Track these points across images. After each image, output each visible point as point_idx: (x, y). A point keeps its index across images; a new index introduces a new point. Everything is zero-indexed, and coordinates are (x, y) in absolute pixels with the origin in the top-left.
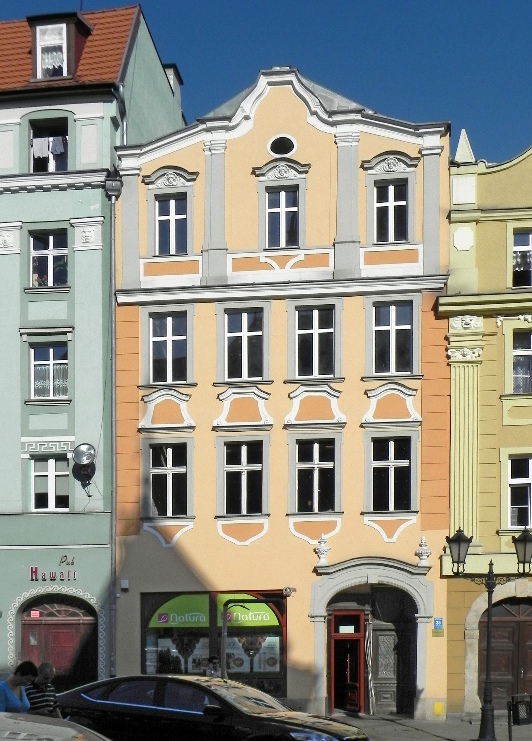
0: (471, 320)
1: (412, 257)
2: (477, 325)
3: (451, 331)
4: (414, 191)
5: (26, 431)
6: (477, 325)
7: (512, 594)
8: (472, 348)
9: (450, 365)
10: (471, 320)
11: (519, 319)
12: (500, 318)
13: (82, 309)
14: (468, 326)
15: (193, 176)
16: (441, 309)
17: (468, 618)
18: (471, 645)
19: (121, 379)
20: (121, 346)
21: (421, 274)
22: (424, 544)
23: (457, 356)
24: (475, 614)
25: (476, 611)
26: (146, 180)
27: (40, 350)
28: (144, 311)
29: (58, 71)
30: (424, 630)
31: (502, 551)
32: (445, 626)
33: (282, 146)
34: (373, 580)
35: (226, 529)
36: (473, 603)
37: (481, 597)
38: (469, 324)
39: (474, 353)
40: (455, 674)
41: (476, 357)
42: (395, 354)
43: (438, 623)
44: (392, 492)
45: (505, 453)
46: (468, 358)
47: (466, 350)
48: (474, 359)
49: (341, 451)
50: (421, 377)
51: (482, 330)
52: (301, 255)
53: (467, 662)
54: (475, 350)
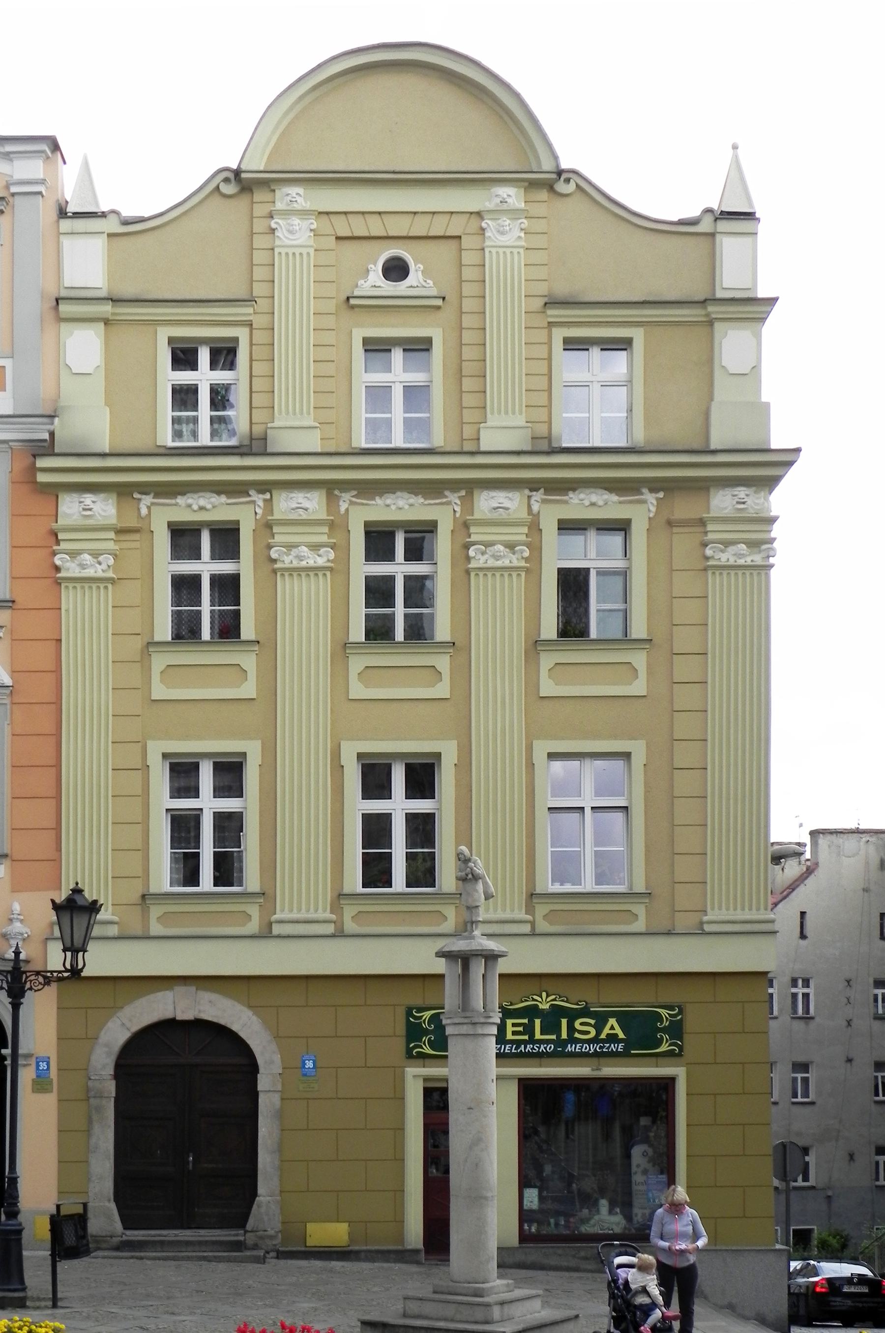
0: (93, 502)
2: (104, 511)
3: (61, 521)
6: (104, 511)
7: (169, 1015)
8: (96, 554)
9: (60, 584)
10: (93, 502)
11: (176, 505)
12: (147, 500)
14: (88, 513)
16: (42, 478)
17: (94, 1058)
18: (99, 1109)
21: (11, 413)
22: (15, 916)
23: (71, 569)
24: (106, 1049)
25: (106, 1045)
31: (152, 933)
32: (54, 1073)
36: (102, 1029)
37: (115, 1018)
38: (90, 510)
39: (100, 563)
40: (71, 1162)
41: (103, 571)
43: (43, 1066)
45: (156, 749)
46: (90, 572)
47: (86, 557)
48: (100, 574)
50: (10, 604)
51: (114, 521)
53: (93, 1141)
54: (101, 558)
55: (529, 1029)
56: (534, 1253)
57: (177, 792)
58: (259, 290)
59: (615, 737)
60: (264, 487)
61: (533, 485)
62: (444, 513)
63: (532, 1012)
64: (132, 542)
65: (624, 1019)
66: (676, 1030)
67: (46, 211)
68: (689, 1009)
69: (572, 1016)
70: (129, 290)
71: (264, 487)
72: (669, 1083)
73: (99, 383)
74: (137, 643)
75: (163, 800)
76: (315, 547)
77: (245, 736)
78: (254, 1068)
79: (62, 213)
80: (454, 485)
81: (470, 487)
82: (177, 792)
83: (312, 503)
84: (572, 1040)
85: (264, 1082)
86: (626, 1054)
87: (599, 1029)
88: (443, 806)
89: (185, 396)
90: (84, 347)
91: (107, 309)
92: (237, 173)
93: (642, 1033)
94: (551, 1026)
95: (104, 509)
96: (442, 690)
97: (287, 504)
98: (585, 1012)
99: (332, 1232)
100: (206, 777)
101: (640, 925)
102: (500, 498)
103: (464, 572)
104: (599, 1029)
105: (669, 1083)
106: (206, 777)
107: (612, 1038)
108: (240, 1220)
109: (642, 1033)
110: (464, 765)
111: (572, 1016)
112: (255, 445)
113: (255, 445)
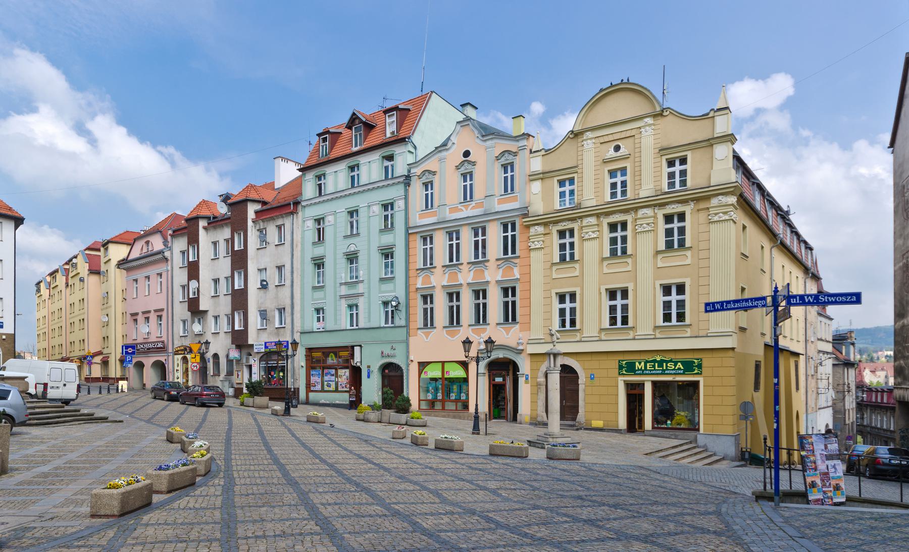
1: (515, 199)
4: (516, 167)
5: (380, 292)
13: (397, 238)
15: (434, 173)
19: (411, 266)
20: (411, 252)
26: (420, 177)
27: (387, 256)
28: (418, 236)
29: (393, 133)
30: (521, 380)
33: (467, 154)
34: (501, 356)
35: (448, 332)
42: (509, 246)
44: (510, 314)
49: (489, 294)
52: (473, 203)
55: (654, 366)
56: (656, 432)
57: (560, 303)
58: (580, 162)
59: (680, 277)
60: (580, 217)
61: (655, 205)
62: (629, 218)
63: (655, 361)
64: (548, 237)
65: (683, 363)
66: (700, 366)
67: (527, 152)
68: (704, 360)
69: (667, 362)
70: (547, 169)
71: (580, 217)
72: (698, 382)
73: (540, 195)
74: (550, 264)
75: (557, 306)
76: (593, 232)
77: (576, 286)
78: (578, 377)
79: (531, 152)
80: (632, 209)
81: (636, 209)
82: (560, 303)
83: (593, 220)
84: (667, 369)
85: (580, 382)
86: (684, 374)
87: (675, 366)
88: (630, 302)
89: (562, 195)
90: (536, 186)
91: (541, 176)
92: (572, 131)
93: (689, 367)
94: (661, 365)
95: (540, 229)
96: (629, 268)
97: (586, 221)
98: (671, 361)
99: (599, 424)
100: (568, 298)
101: (688, 335)
102: (645, 211)
103: (636, 233)
104: (675, 366)
105: (698, 382)
106: (568, 298)
107: (679, 369)
108: (574, 419)
109: (689, 367)
110: (635, 290)
111: (667, 362)
112: (579, 207)
113: (579, 207)
